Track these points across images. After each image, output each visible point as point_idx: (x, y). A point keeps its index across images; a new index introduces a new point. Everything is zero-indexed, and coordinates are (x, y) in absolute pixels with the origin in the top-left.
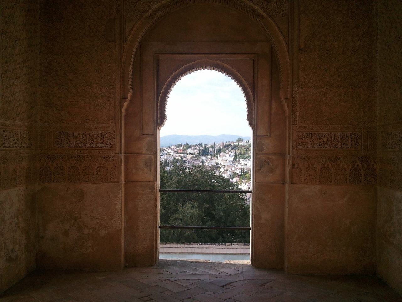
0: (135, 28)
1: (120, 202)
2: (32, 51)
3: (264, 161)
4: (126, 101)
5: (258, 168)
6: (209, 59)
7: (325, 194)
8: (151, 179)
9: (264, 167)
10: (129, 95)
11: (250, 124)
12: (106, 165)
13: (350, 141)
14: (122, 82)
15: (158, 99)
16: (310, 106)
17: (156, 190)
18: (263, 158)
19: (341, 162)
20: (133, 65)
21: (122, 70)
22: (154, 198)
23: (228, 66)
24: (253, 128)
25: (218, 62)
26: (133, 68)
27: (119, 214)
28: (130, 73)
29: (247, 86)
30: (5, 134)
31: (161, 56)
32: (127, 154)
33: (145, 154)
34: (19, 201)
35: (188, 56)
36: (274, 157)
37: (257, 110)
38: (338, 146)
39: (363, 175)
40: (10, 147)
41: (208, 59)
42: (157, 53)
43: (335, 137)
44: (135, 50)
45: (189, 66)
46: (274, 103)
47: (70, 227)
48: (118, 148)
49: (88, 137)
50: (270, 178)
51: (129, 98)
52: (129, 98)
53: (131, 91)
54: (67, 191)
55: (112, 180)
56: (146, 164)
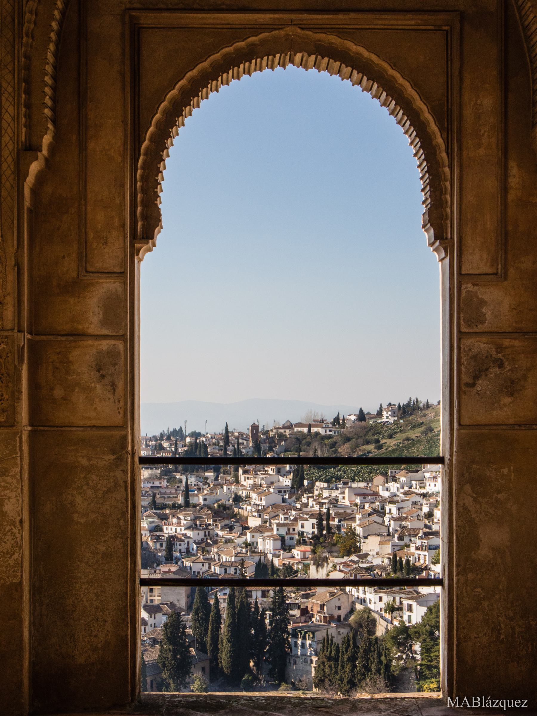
1: (19, 491)
3: (487, 357)
4: (36, 159)
5: (466, 379)
6: (303, 29)
8: (117, 419)
9: (486, 375)
10: (47, 140)
14: (23, 96)
17: (133, 455)
18: (483, 346)
20: (57, 45)
21: (23, 59)
22: (126, 482)
23: (366, 53)
27: (16, 531)
28: (49, 69)
29: (427, 116)
32: (38, 338)
36: (517, 343)
37: (461, 189)
41: (299, 31)
42: (134, 9)
45: (237, 50)
46: (514, 169)
48: (9, 313)
50: (506, 411)
52: (45, 151)
53: (50, 126)
56: (99, 371)
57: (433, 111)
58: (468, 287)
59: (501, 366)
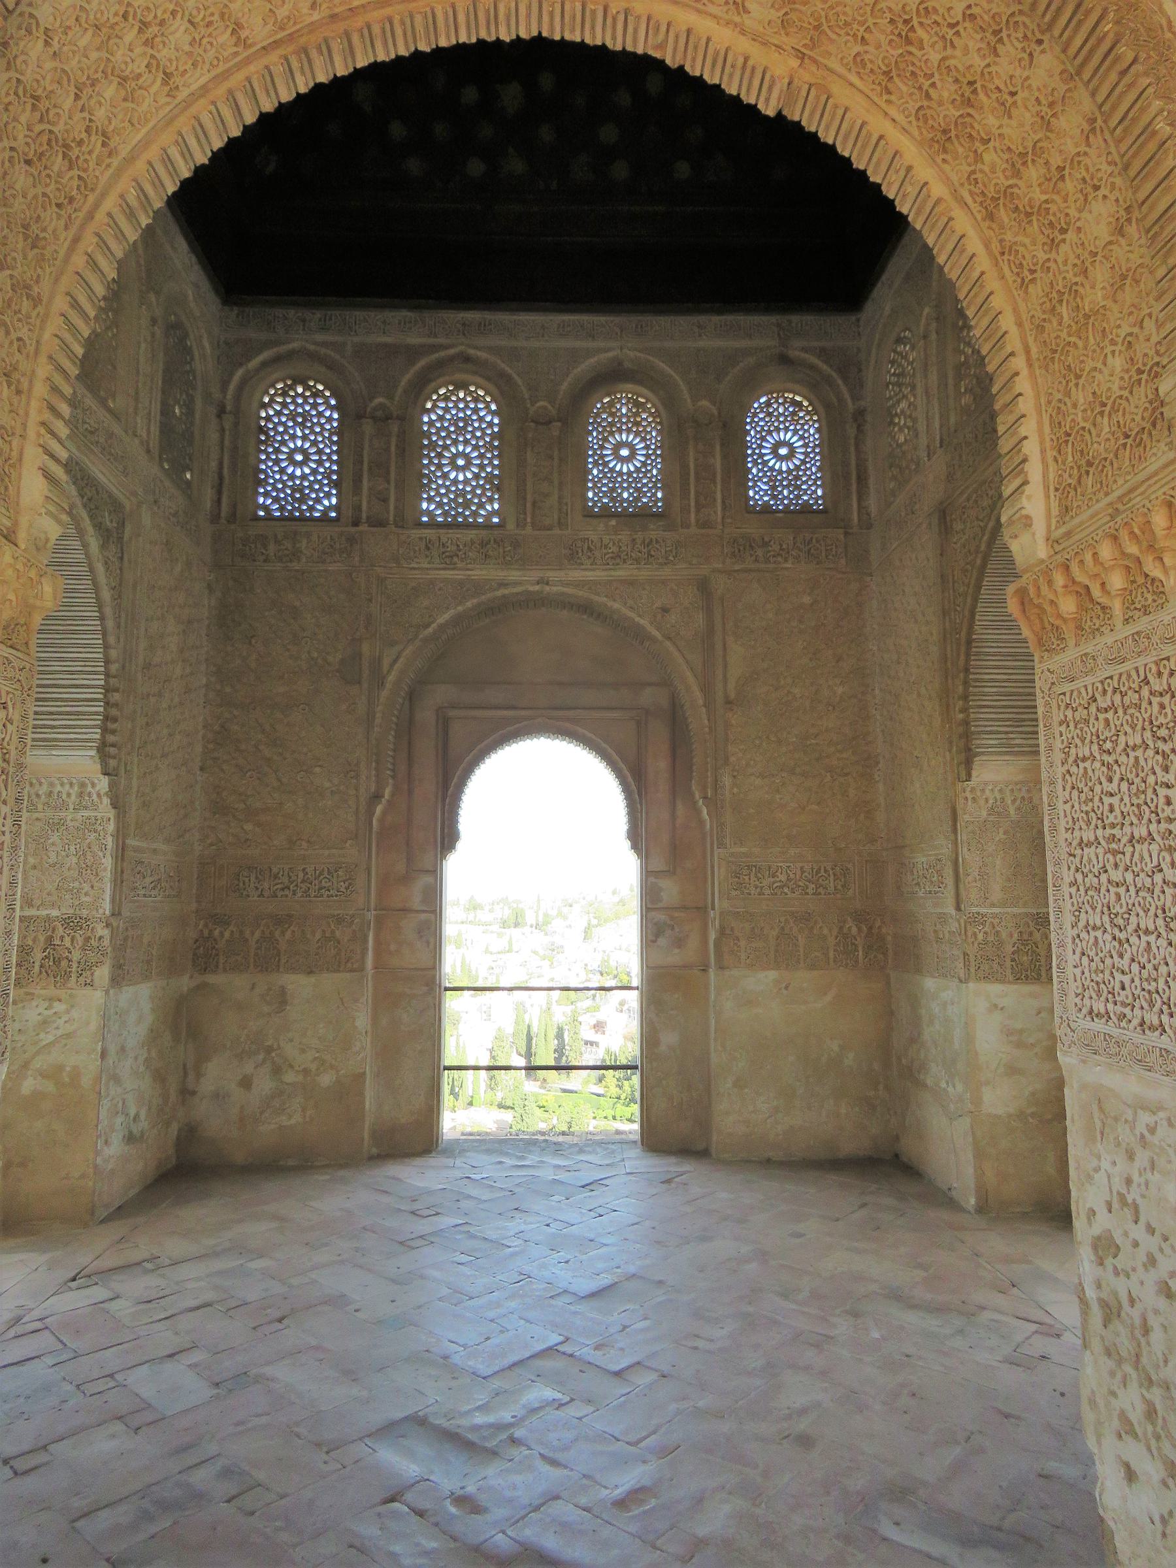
0: (401, 660)
2: (191, 701)
5: (651, 937)
7: (786, 988)
10: (387, 793)
11: (635, 846)
12: (338, 933)
13: (832, 877)
15: (444, 800)
16: (752, 811)
19: (816, 922)
24: (639, 855)
25: (567, 725)
26: (395, 737)
28: (391, 746)
30: (139, 868)
31: (452, 713)
33: (417, 911)
34: (153, 1010)
35: (511, 713)
36: (682, 914)
38: (810, 891)
39: (860, 949)
40: (145, 896)
43: (803, 872)
44: (400, 700)
46: (680, 807)
47: (256, 1067)
49: (301, 875)
50: (675, 958)
51: (387, 796)
52: (387, 796)
54: (253, 988)
55: (349, 965)
57: (631, 770)
58: (652, 879)
59: (673, 929)
